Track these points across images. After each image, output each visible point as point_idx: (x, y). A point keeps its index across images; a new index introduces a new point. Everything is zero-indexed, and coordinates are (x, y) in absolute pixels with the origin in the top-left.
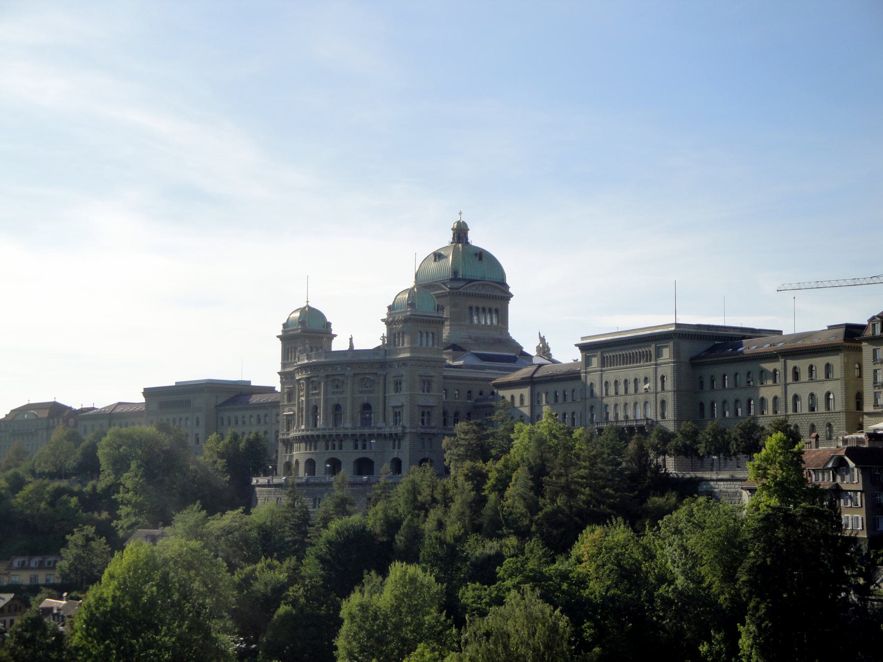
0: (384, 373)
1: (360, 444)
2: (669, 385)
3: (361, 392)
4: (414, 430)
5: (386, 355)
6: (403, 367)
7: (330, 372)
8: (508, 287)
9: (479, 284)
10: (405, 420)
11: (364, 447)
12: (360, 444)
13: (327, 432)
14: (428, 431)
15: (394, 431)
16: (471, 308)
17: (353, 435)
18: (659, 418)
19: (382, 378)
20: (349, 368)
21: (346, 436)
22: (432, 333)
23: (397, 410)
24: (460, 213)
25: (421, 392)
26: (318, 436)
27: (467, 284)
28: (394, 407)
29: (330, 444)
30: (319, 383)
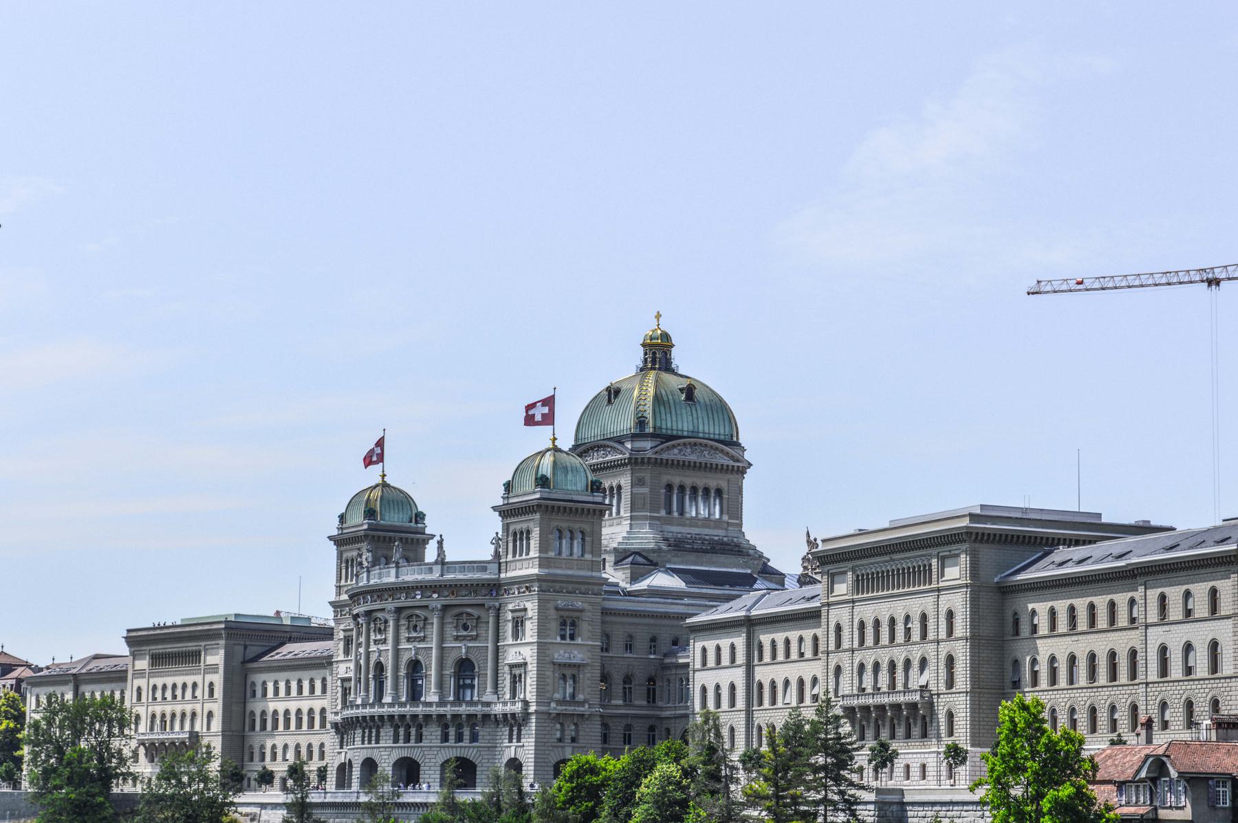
0: (497, 604)
1: (452, 732)
2: (961, 628)
3: (457, 638)
4: (543, 708)
5: (500, 572)
6: (527, 593)
7: (403, 601)
8: (744, 450)
9: (684, 444)
10: (529, 690)
11: (459, 738)
12: (452, 732)
13: (396, 710)
14: (571, 709)
15: (509, 708)
16: (669, 487)
17: (441, 717)
18: (943, 688)
19: (492, 613)
20: (435, 596)
21: (428, 717)
22: (582, 532)
23: (517, 672)
24: (658, 316)
25: (559, 639)
26: (381, 717)
27: (662, 443)
28: (512, 666)
29: (402, 731)
30: (386, 622)
